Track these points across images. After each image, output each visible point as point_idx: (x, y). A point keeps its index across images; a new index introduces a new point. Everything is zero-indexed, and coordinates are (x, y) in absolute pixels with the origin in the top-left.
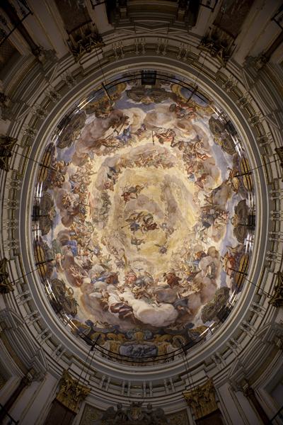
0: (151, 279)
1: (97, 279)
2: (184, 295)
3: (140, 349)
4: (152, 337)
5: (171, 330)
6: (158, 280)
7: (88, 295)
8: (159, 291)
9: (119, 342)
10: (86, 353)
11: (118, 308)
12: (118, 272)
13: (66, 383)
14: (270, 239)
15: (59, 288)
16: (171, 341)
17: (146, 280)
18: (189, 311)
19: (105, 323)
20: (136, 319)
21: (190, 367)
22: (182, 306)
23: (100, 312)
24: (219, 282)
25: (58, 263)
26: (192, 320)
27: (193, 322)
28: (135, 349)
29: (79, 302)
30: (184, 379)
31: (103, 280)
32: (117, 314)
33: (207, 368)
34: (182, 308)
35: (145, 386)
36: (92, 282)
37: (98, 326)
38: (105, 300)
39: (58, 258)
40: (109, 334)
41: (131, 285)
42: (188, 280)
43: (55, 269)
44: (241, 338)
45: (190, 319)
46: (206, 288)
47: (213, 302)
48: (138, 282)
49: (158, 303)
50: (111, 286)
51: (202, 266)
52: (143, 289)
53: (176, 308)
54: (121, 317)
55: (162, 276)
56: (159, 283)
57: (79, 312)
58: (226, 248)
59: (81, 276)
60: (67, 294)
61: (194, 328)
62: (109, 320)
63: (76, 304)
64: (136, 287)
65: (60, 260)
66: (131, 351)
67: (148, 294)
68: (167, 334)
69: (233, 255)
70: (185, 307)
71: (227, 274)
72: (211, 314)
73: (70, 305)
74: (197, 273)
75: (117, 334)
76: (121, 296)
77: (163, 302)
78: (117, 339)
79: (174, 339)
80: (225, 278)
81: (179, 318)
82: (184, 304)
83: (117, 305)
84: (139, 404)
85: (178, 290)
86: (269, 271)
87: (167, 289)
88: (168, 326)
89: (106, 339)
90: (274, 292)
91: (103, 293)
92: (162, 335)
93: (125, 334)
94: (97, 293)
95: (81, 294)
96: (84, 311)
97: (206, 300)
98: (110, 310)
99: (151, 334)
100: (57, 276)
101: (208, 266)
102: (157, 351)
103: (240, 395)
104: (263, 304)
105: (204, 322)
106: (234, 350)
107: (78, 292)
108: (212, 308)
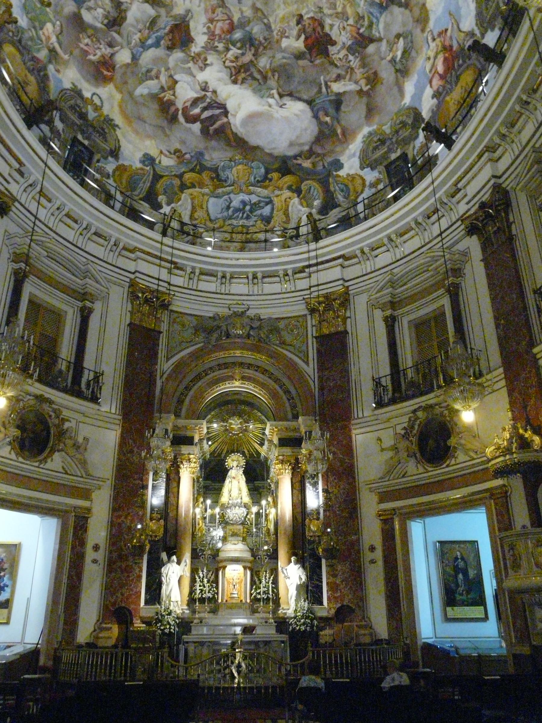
0: (268, 27)
1: (143, 45)
2: (337, 87)
3: (244, 203)
4: (266, 178)
5: (300, 165)
6: (283, 34)
7: (131, 94)
8: (280, 66)
9: (206, 190)
10: (157, 242)
11: (197, 111)
12: (188, 11)
13: (138, 297)
14: (517, 108)
15: (72, 108)
16: (298, 191)
17: (257, 30)
18: (339, 131)
19: (177, 151)
20: (235, 135)
21: (320, 260)
22: (327, 115)
23: (162, 128)
24: (409, 88)
25: (52, 51)
26: (342, 152)
27: (343, 159)
28: (236, 203)
29: (118, 120)
30: (310, 273)
31: (157, 44)
32: (197, 127)
33: (347, 263)
34: (328, 119)
35: (251, 277)
36: (135, 58)
37: (167, 162)
38: (168, 96)
39: (48, 38)
40: (187, 176)
41: (221, 46)
42: (351, 50)
43: (51, 68)
44: (406, 237)
45: (338, 149)
46: (381, 89)
47: (387, 129)
48: (238, 35)
49: (281, 96)
50: (178, 55)
51: (387, 26)
52: (248, 57)
53: (316, 116)
54: (205, 132)
55: (293, 22)
56: (285, 43)
57: (123, 143)
58: (448, 15)
59: (109, 51)
60: (92, 115)
61: (342, 173)
62: (183, 142)
63: (115, 126)
64: (234, 51)
65: (54, 39)
66: (228, 207)
67: (260, 72)
68: (294, 174)
69: (455, 47)
70: (333, 118)
71: (431, 82)
72: (378, 154)
73: (103, 134)
74: (372, 40)
75: (200, 173)
76: (202, 76)
77: (291, 95)
78: (201, 185)
79: (304, 187)
80: (424, 88)
81: (320, 139)
82: (332, 111)
83: (195, 102)
84: (243, 313)
85: (323, 70)
86: (490, 160)
87: (301, 62)
88: (295, 157)
89: (183, 187)
90: (477, 206)
91: (163, 79)
92: (283, 175)
93: (215, 170)
94: (150, 83)
95: (118, 96)
96: (132, 136)
97: (377, 119)
98: (181, 119)
99: (263, 170)
100: (60, 81)
101: (398, 36)
102: (273, 209)
103: (378, 315)
104: (458, 203)
105: (362, 168)
106: (391, 250)
107: (111, 97)
108: (382, 142)
